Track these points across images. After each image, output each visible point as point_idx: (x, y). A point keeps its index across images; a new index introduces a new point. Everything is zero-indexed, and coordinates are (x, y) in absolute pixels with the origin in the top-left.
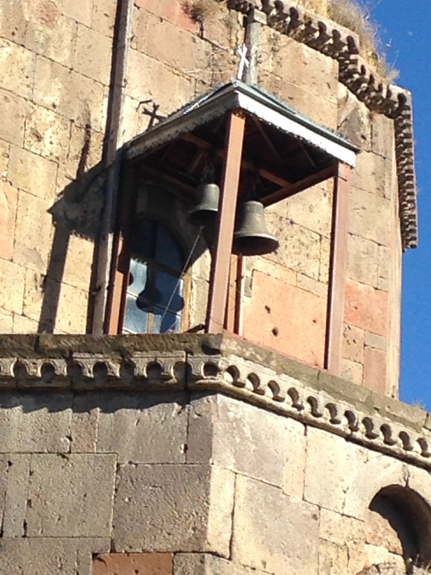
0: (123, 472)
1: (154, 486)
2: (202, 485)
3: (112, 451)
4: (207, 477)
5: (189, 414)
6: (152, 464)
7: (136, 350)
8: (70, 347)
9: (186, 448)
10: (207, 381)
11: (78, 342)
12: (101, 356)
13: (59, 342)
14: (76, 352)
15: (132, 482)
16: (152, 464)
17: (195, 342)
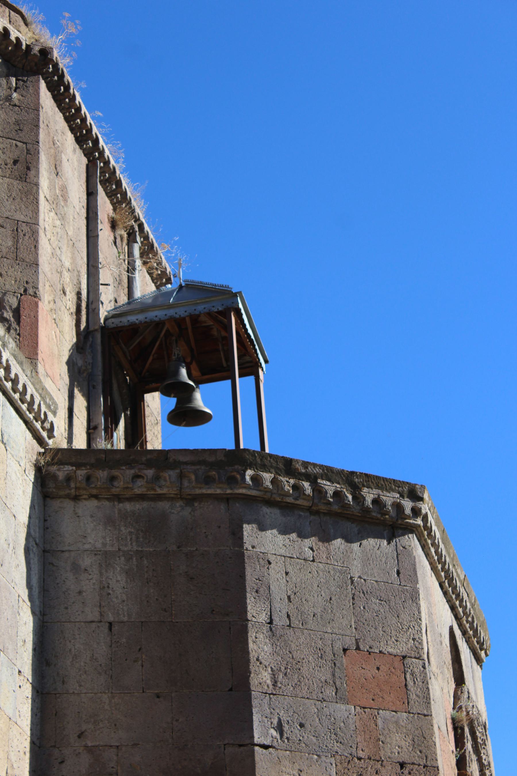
0: (356, 584)
1: (380, 600)
2: (415, 604)
3: (345, 566)
4: (418, 600)
5: (396, 545)
6: (376, 581)
7: (364, 486)
8: (315, 473)
9: (398, 573)
10: (411, 521)
11: (321, 471)
12: (338, 486)
13: (307, 468)
14: (320, 478)
15: (363, 593)
16: (376, 581)
17: (406, 488)
